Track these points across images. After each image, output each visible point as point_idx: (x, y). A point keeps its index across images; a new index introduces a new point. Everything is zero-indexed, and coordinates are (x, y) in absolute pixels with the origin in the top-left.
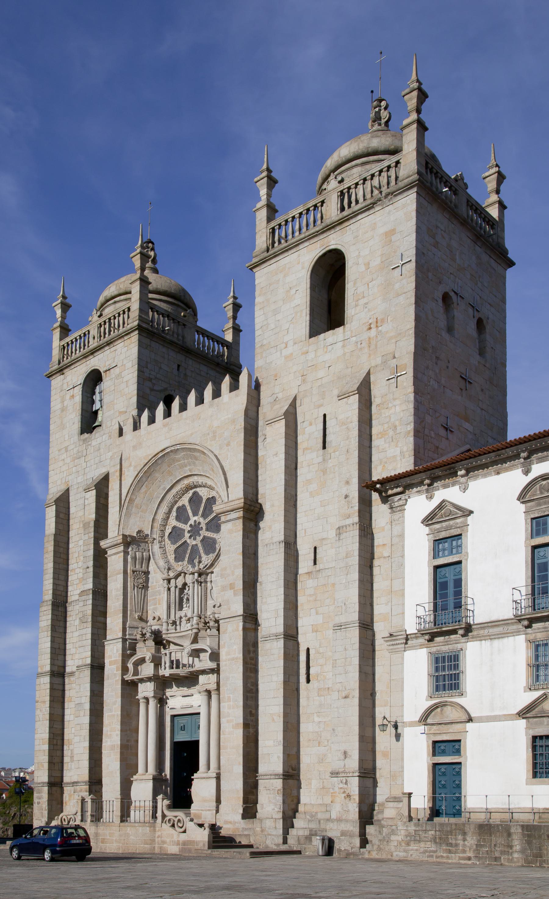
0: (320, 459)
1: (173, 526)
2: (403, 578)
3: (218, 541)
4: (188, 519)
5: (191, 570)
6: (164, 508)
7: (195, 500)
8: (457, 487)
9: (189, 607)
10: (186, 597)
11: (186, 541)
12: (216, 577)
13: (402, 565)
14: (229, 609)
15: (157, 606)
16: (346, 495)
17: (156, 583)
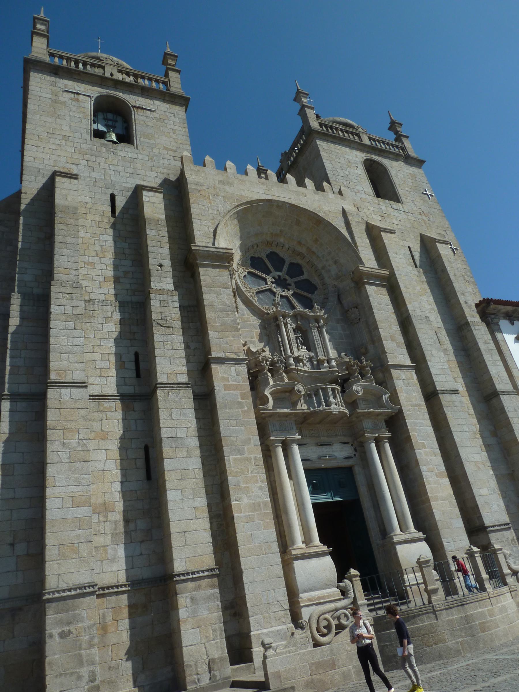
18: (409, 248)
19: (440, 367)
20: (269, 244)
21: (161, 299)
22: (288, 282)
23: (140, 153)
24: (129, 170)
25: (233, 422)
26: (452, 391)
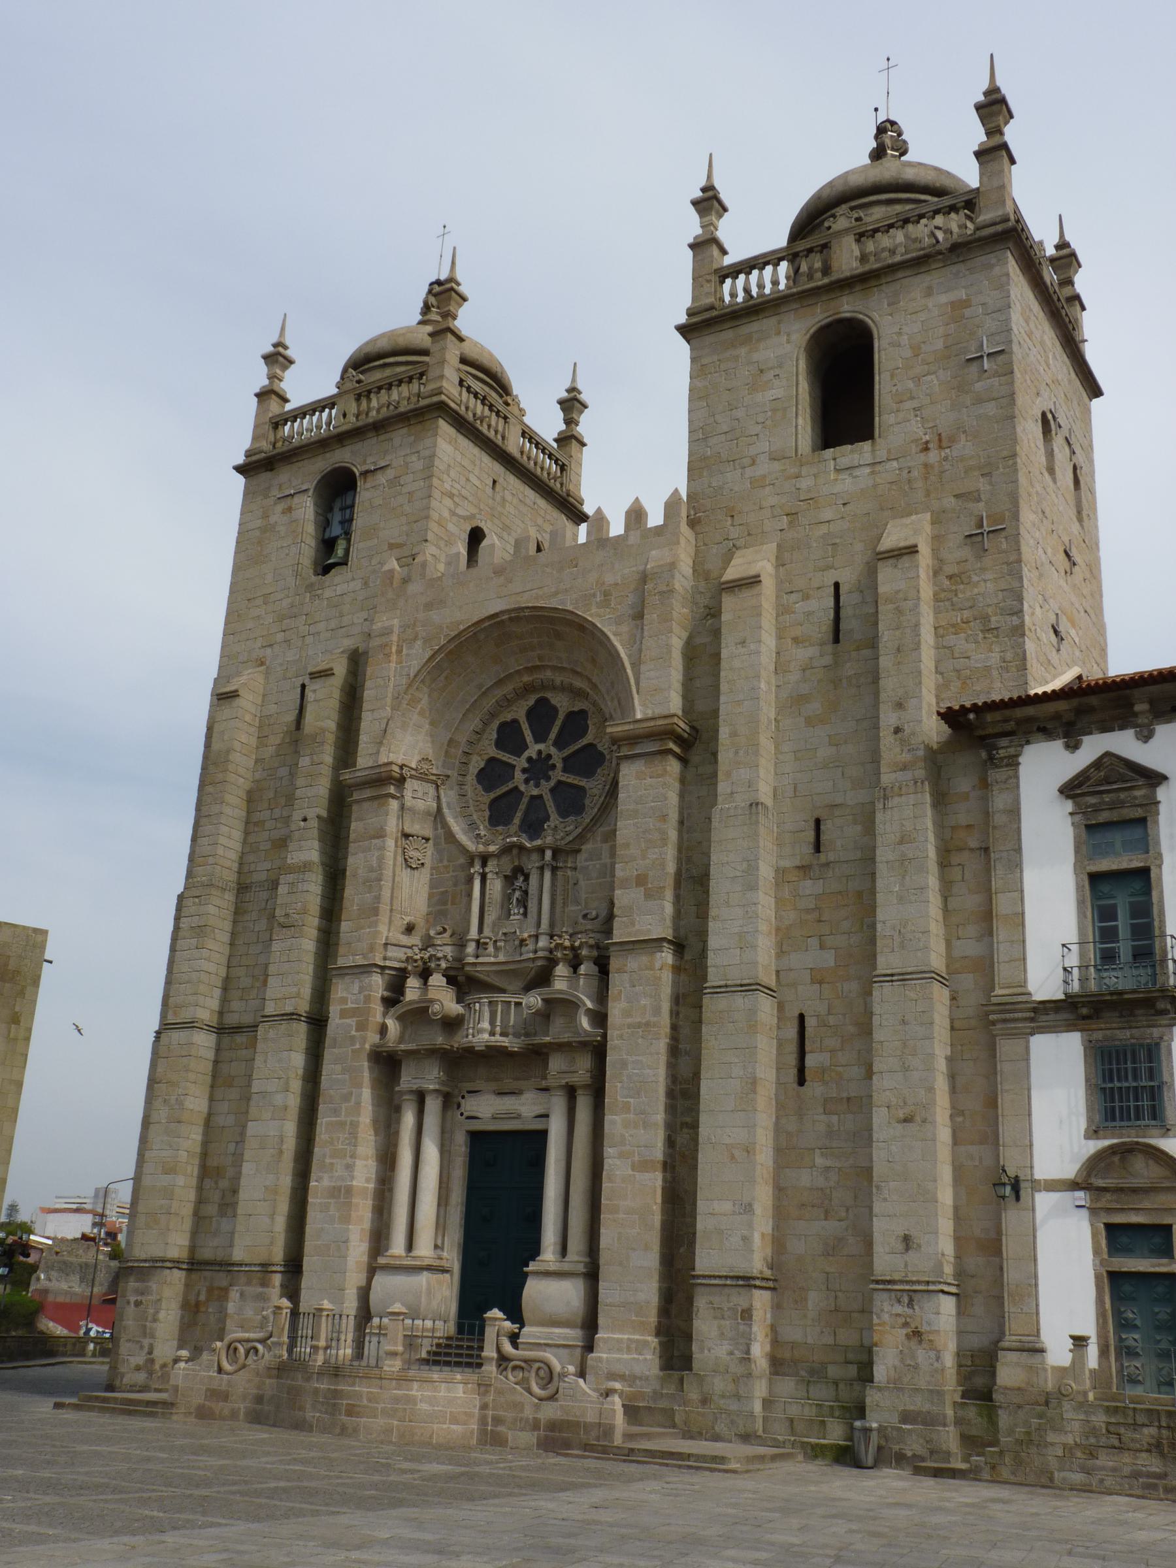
0: (828, 660)
1: (486, 757)
2: (1022, 891)
3: (589, 792)
9: (525, 914)
10: (517, 894)
12: (586, 860)
14: (633, 924)
15: (449, 906)
16: (898, 728)
17: (448, 861)
18: (837, 586)
19: (736, 930)
20: (528, 689)
21: (291, 881)
22: (550, 763)
23: (353, 579)
24: (333, 624)
25: (338, 1068)
26: (742, 985)
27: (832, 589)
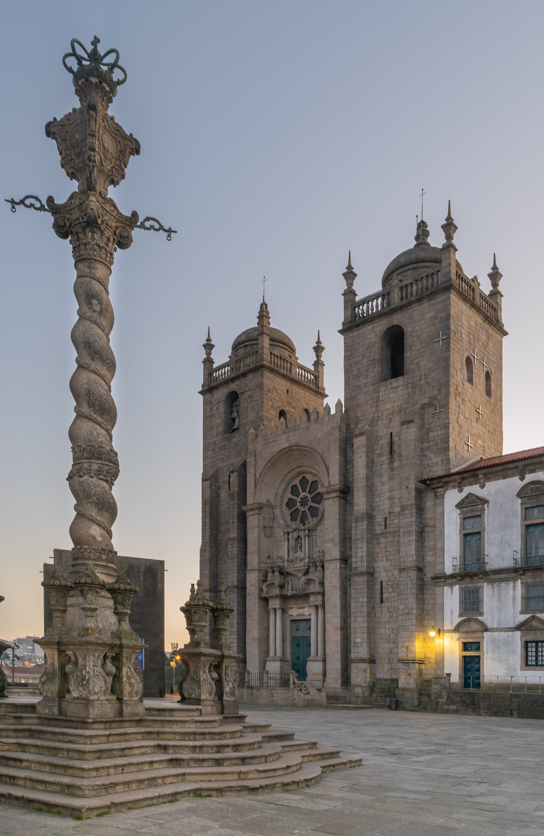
0: (389, 461)
4: (299, 494)
5: (303, 528)
6: (283, 486)
7: (304, 481)
8: (478, 486)
11: (298, 509)
13: (442, 533)
27: (389, 435)
